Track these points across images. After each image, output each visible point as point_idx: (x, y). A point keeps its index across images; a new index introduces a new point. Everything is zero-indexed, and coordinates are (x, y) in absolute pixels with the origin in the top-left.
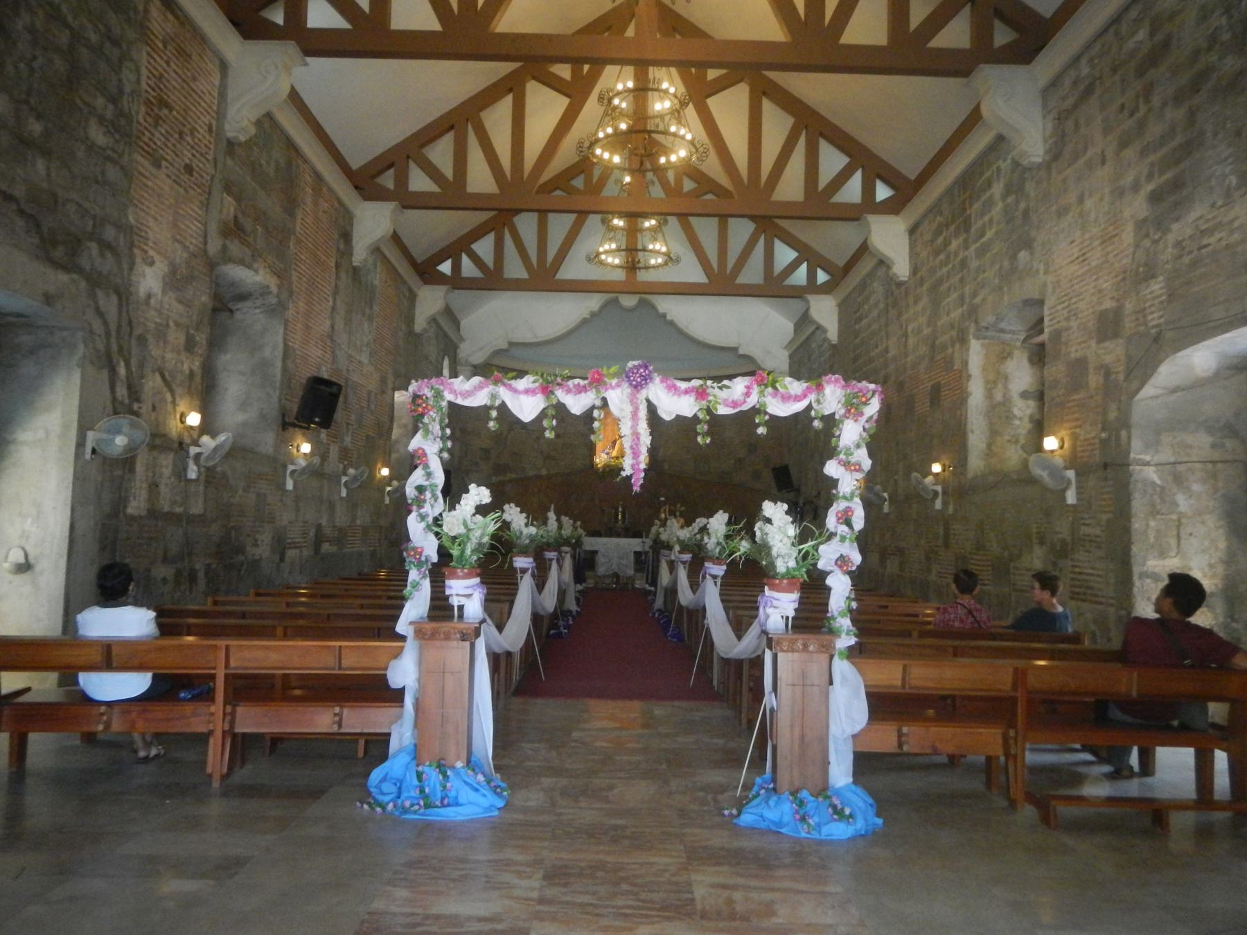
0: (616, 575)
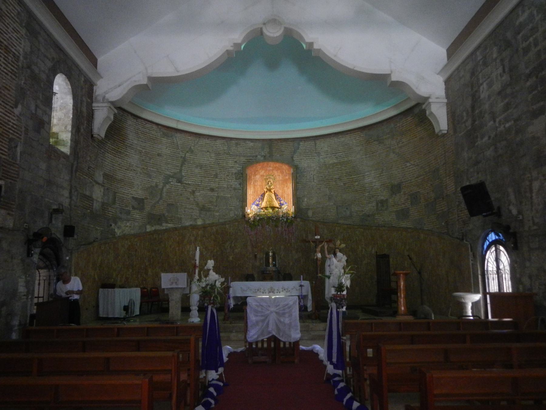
0: (274, 339)
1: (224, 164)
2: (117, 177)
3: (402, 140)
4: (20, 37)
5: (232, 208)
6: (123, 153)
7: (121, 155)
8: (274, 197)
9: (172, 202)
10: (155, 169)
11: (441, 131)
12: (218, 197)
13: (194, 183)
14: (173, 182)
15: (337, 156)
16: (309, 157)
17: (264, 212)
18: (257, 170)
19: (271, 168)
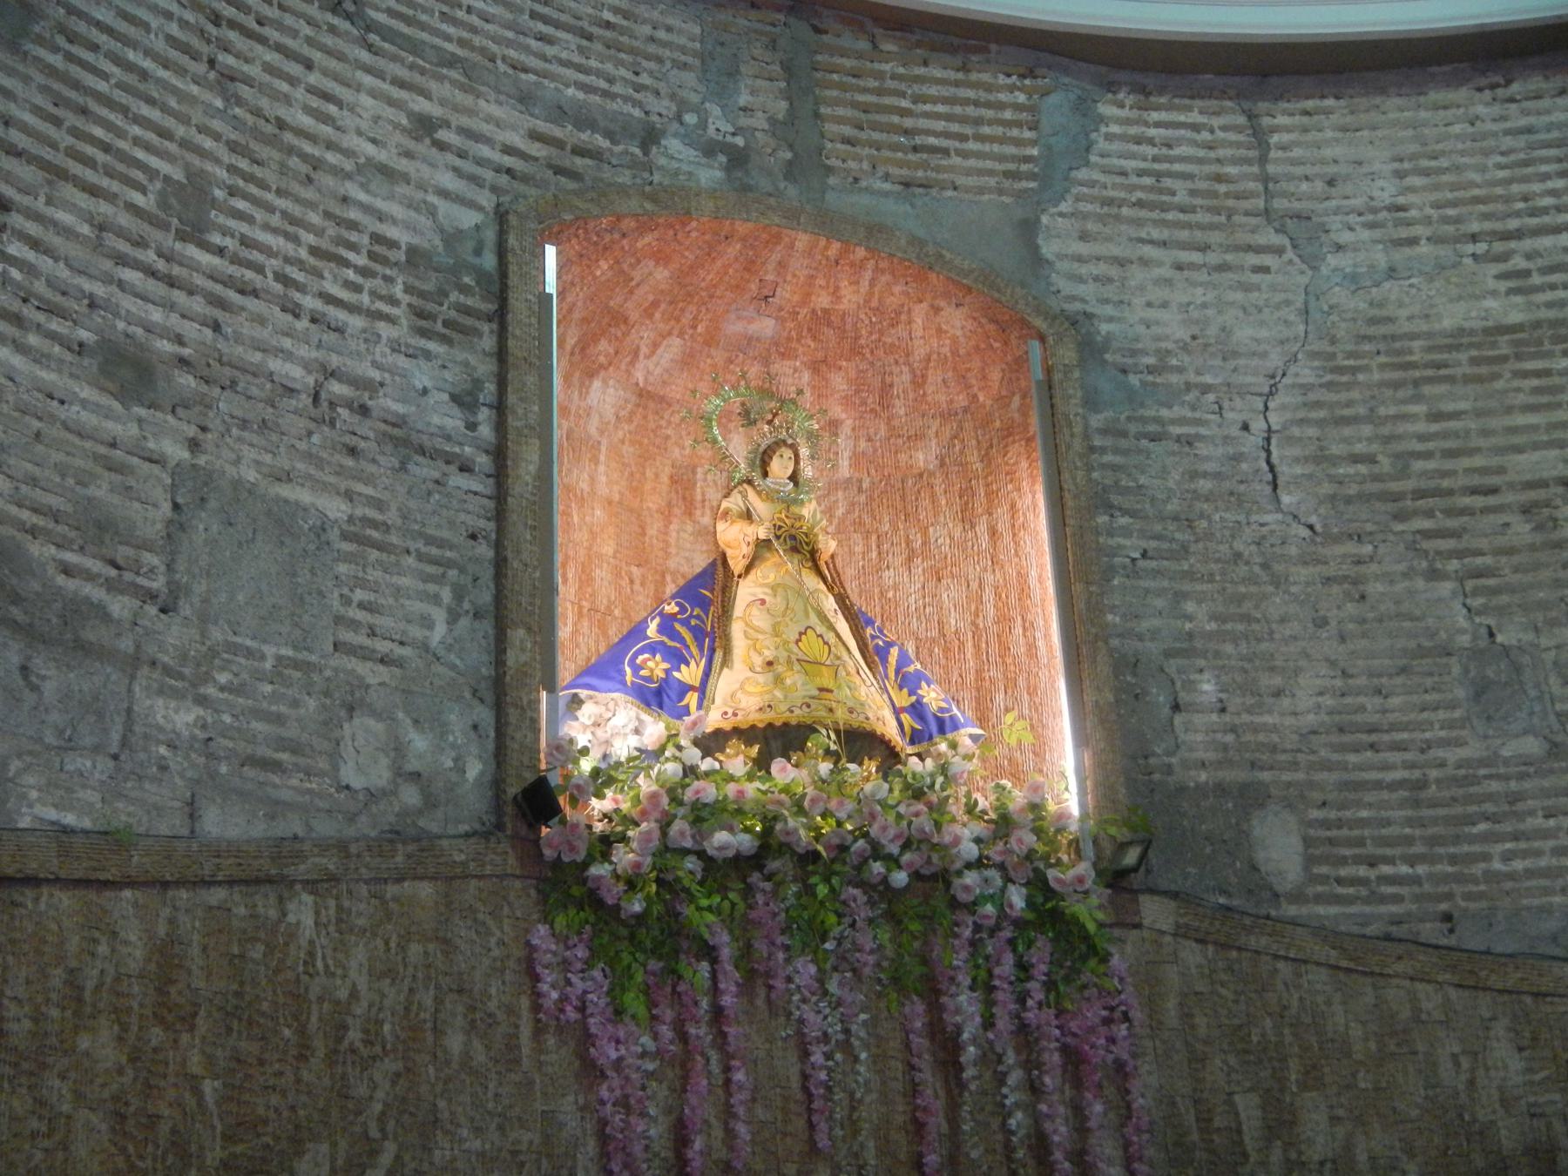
1: (287, 100)
15: (1519, 262)
16: (1204, 248)
19: (766, 327)
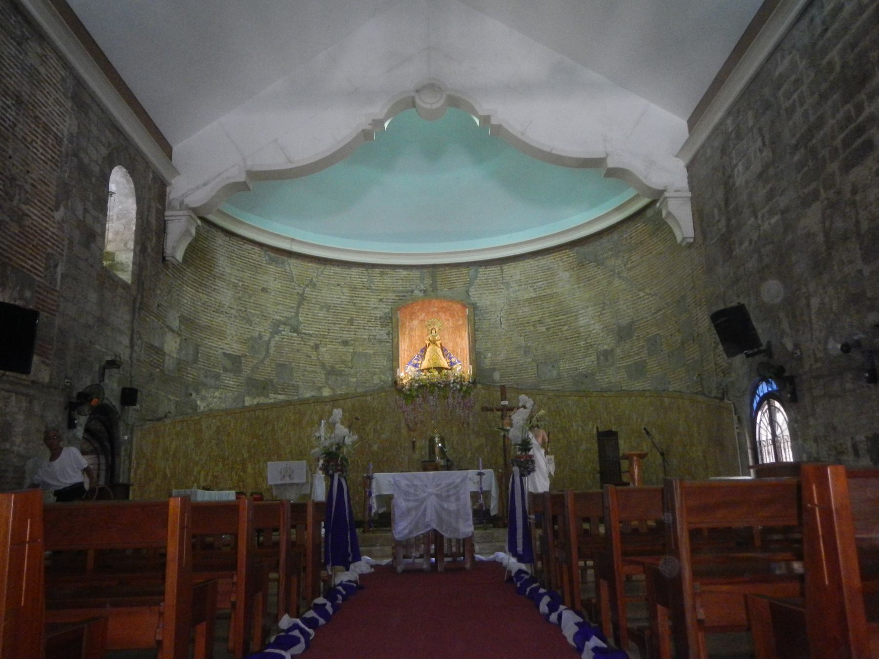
0: (436, 537)
2: (201, 322)
3: (632, 258)
4: (63, 112)
5: (377, 370)
6: (210, 286)
7: (207, 290)
8: (440, 353)
9: (284, 361)
10: (259, 311)
11: (684, 239)
12: (354, 354)
13: (317, 333)
14: (284, 331)
15: (535, 287)
16: (493, 290)
17: (425, 375)
18: (415, 313)
